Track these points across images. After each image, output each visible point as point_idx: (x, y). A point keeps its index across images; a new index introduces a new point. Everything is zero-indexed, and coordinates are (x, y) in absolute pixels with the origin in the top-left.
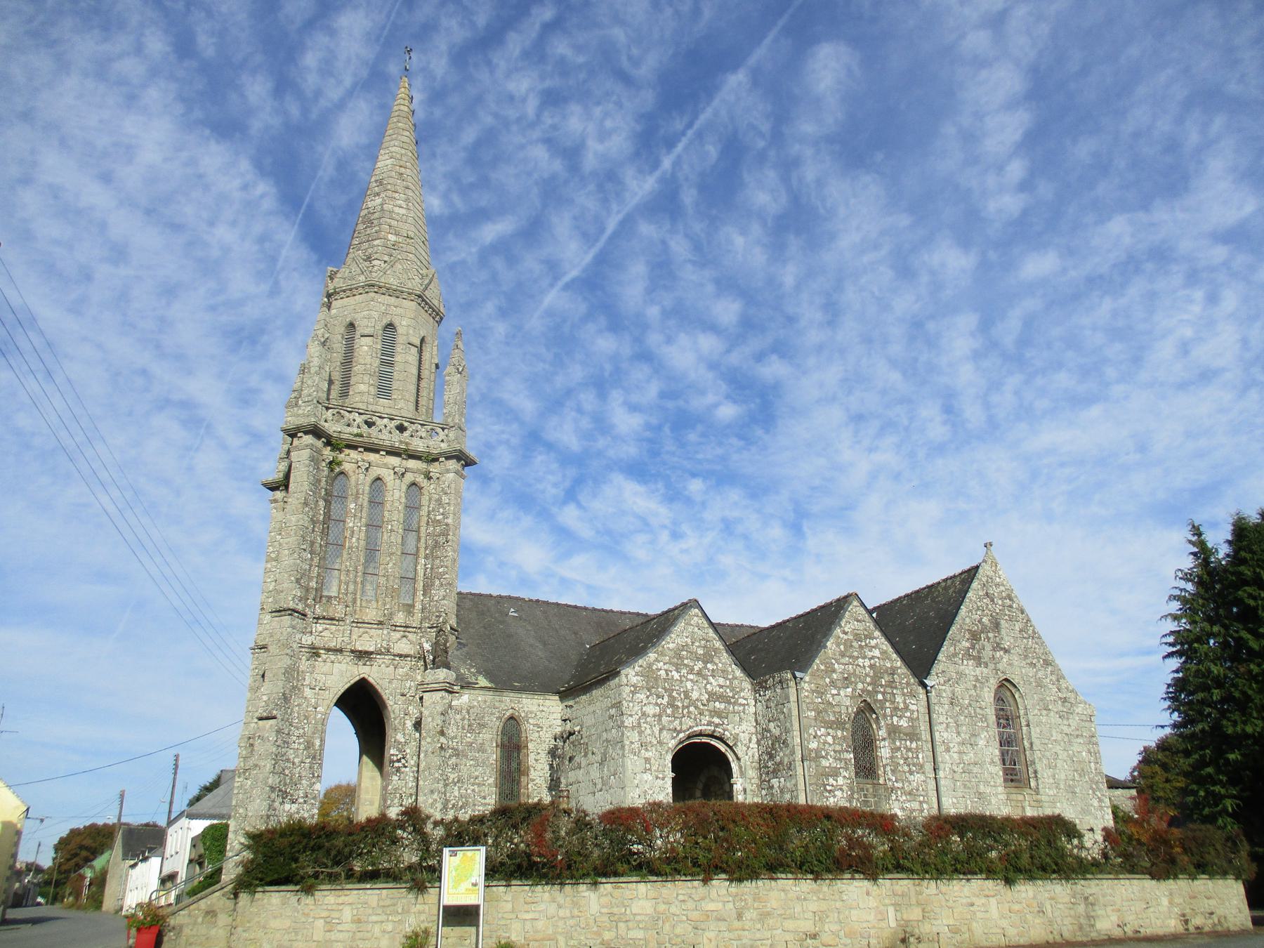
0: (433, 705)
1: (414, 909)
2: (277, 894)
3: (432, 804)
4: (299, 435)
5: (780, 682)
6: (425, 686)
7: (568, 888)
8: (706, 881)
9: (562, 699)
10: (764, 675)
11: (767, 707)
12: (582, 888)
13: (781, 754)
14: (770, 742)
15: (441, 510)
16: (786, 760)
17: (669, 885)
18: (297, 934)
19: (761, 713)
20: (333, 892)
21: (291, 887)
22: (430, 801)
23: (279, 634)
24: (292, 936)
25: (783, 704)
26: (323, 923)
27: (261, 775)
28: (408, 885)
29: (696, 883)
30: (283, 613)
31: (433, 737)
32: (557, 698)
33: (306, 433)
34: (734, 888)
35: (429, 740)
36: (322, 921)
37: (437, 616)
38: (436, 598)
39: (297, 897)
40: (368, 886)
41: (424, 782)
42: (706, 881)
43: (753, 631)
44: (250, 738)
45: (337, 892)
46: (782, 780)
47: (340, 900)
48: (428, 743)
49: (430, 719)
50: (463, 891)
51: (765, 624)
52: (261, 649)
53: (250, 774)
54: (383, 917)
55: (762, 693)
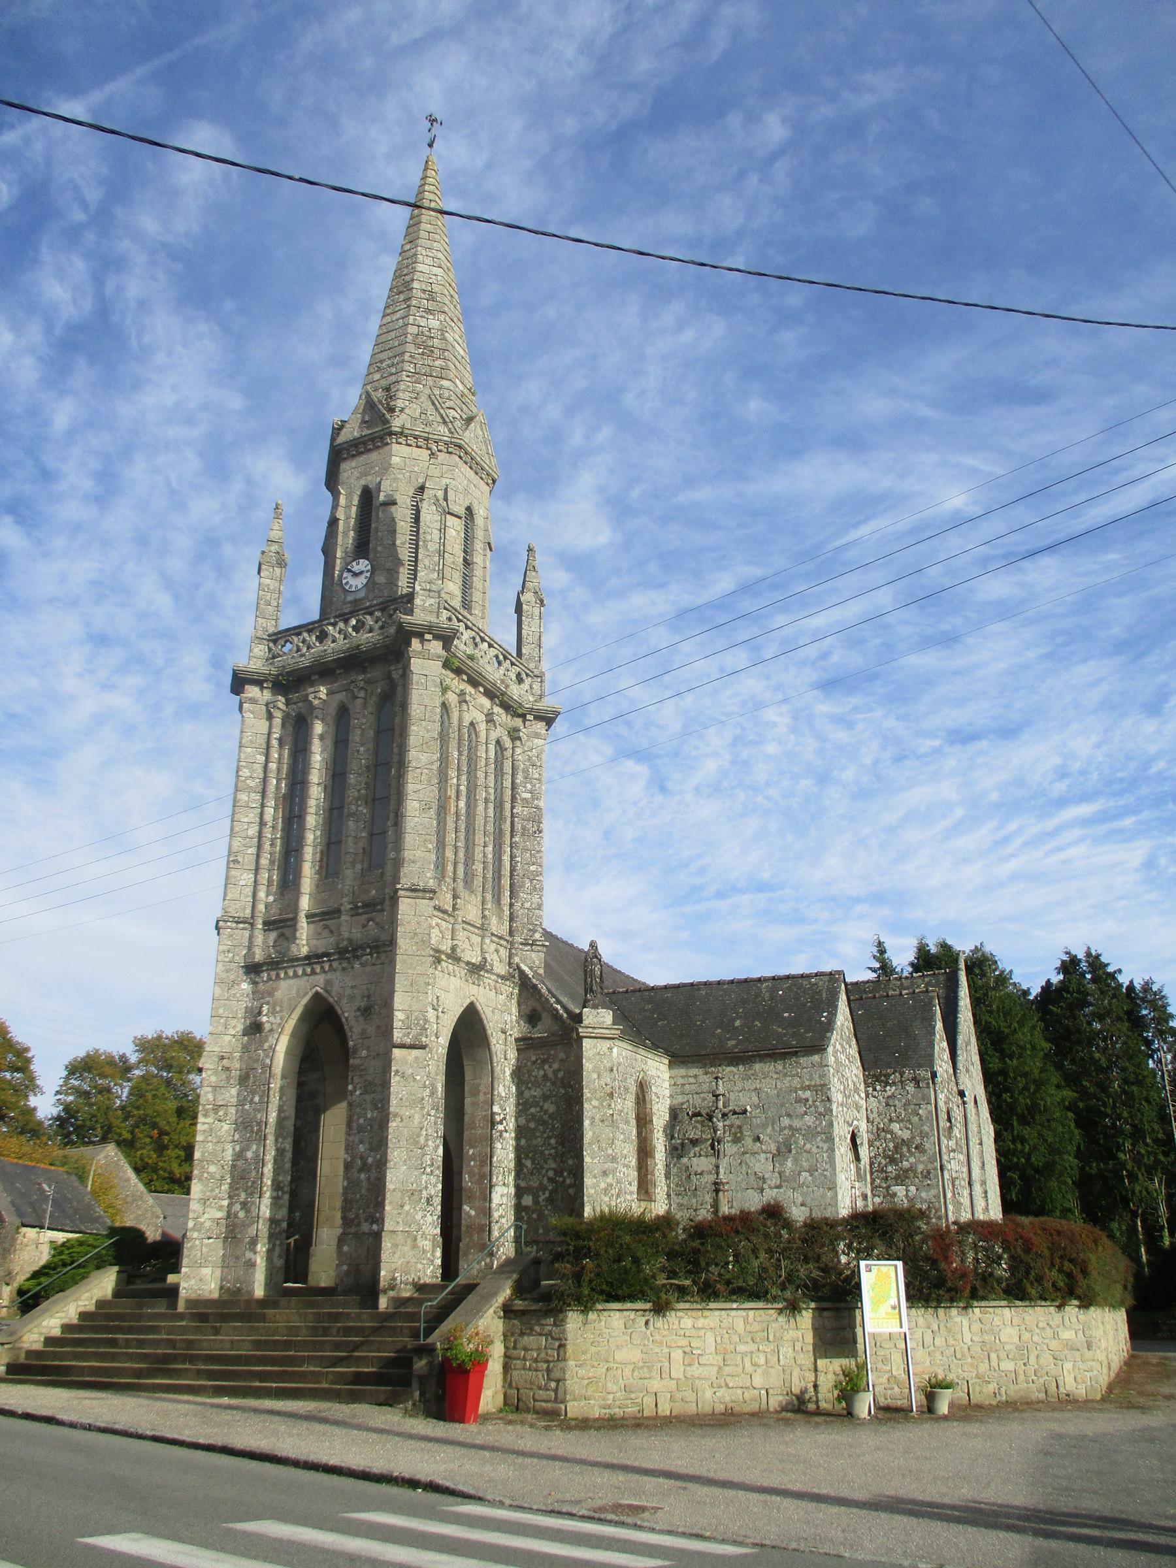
0: (598, 1058)
1: (787, 1336)
2: (617, 1313)
3: (606, 1189)
4: (428, 637)
5: (914, 1079)
6: (590, 1030)
7: (941, 1311)
8: (1060, 1307)
9: (671, 1065)
10: (889, 1065)
11: (887, 1105)
12: (954, 1312)
13: (912, 1160)
14: (891, 1145)
15: (529, 786)
16: (920, 1168)
17: (1030, 1310)
18: (650, 1369)
19: (875, 1110)
20: (690, 1313)
21: (639, 1305)
22: (603, 1185)
23: (414, 923)
24: (645, 1372)
25: (919, 1105)
26: (682, 1355)
27: (406, 1131)
28: (780, 1306)
29: (1052, 1308)
30: (420, 894)
31: (600, 1099)
32: (667, 1062)
33: (436, 637)
34: (1083, 1315)
35: (595, 1103)
36: (680, 1351)
37: (530, 930)
38: (527, 905)
39: (644, 1320)
40: (735, 1305)
41: (593, 1158)
42: (1060, 1307)
43: (638, 987)
44: (222, 1058)
45: (694, 1313)
46: (913, 1188)
47: (701, 1322)
48: (594, 1107)
49: (595, 1076)
50: (884, 1315)
51: (651, 983)
52: (237, 922)
53: (226, 1114)
54: (753, 1347)
55: (878, 1088)
